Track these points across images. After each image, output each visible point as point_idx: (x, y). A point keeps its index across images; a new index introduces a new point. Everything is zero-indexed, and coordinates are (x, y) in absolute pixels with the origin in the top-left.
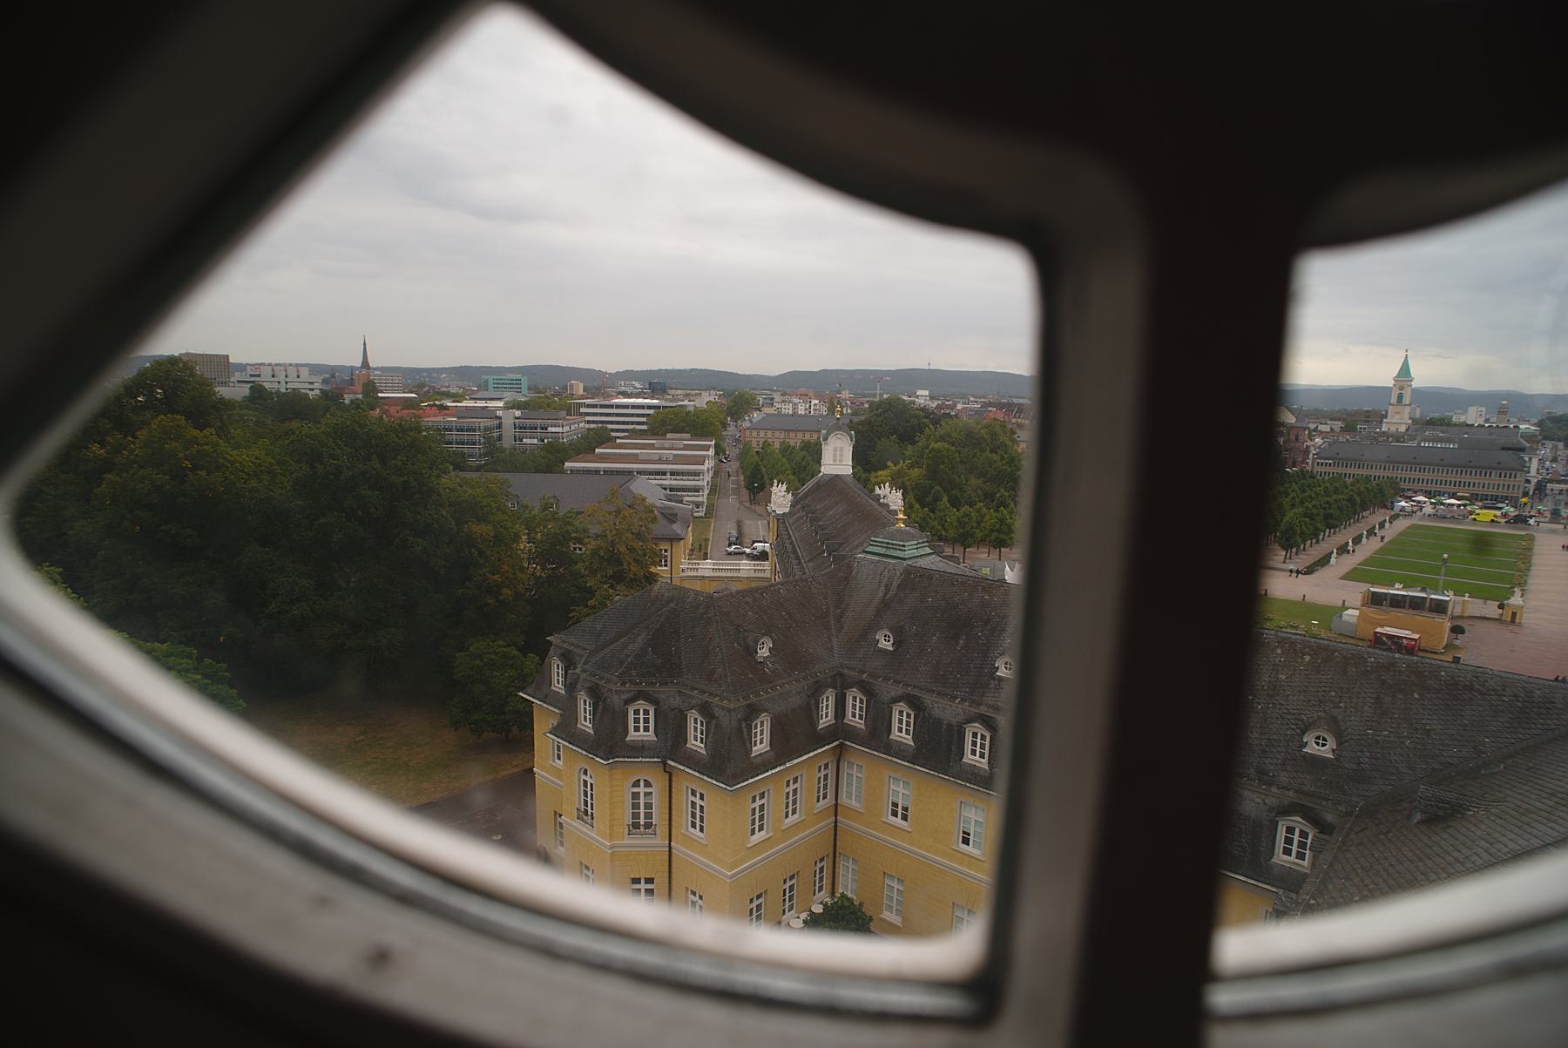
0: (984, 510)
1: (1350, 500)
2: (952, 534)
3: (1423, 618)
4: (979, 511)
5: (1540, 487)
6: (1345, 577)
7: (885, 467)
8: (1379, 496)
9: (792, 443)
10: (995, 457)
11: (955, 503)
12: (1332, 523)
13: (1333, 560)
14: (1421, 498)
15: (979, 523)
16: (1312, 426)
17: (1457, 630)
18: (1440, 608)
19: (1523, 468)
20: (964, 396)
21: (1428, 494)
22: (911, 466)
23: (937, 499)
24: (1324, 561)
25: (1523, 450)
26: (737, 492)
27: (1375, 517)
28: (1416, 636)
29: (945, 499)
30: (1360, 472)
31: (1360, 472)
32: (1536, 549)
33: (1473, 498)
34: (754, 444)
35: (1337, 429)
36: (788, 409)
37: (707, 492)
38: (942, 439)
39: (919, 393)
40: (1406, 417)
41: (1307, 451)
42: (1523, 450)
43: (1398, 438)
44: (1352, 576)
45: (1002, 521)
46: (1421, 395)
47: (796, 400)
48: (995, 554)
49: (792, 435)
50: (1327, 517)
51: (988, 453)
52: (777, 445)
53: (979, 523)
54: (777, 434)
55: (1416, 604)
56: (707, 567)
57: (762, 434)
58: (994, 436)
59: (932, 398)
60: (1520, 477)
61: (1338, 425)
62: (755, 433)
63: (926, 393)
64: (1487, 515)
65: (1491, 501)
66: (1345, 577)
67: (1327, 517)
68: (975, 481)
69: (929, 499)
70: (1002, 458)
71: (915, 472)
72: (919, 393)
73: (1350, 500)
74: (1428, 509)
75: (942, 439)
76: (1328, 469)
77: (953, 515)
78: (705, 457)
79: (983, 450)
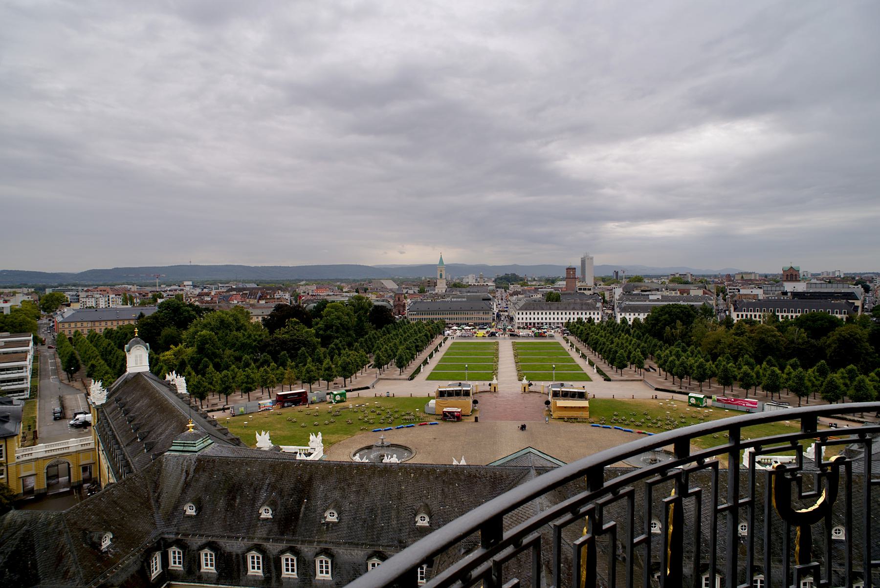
0: (236, 370)
1: (426, 335)
2: (218, 388)
3: (462, 400)
4: (233, 370)
5: (498, 316)
6: (428, 379)
7: (168, 349)
8: (438, 329)
9: (98, 331)
10: (240, 335)
11: (218, 367)
12: (419, 349)
14: (455, 328)
15: (233, 378)
16: (405, 291)
17: (475, 402)
18: (467, 394)
19: (491, 309)
20: (214, 283)
21: (458, 325)
22: (187, 346)
23: (206, 366)
24: (418, 371)
25: (490, 299)
26: (56, 372)
27: (438, 340)
28: (459, 410)
29: (211, 366)
32: (501, 349)
33: (475, 325)
34: (66, 333)
35: (416, 291)
36: (91, 303)
37: (29, 379)
38: (205, 326)
39: (186, 283)
41: (404, 306)
42: (490, 299)
43: (443, 297)
45: (248, 376)
46: (451, 268)
47: (98, 296)
48: (245, 396)
49: (97, 324)
50: (417, 346)
51: (235, 333)
52: (86, 331)
53: (233, 378)
54: (85, 324)
55: (458, 393)
56: (40, 450)
57: (73, 325)
58: (237, 320)
60: (491, 313)
61: (416, 289)
62: (66, 325)
63: (190, 283)
64: (481, 333)
65: (483, 325)
66: (428, 379)
67: (417, 346)
68: (228, 352)
69: (201, 367)
70: (244, 335)
71: (190, 350)
72: (186, 283)
73: (426, 335)
74: (458, 333)
75: (205, 326)
77: (218, 376)
78: (26, 352)
79: (231, 330)
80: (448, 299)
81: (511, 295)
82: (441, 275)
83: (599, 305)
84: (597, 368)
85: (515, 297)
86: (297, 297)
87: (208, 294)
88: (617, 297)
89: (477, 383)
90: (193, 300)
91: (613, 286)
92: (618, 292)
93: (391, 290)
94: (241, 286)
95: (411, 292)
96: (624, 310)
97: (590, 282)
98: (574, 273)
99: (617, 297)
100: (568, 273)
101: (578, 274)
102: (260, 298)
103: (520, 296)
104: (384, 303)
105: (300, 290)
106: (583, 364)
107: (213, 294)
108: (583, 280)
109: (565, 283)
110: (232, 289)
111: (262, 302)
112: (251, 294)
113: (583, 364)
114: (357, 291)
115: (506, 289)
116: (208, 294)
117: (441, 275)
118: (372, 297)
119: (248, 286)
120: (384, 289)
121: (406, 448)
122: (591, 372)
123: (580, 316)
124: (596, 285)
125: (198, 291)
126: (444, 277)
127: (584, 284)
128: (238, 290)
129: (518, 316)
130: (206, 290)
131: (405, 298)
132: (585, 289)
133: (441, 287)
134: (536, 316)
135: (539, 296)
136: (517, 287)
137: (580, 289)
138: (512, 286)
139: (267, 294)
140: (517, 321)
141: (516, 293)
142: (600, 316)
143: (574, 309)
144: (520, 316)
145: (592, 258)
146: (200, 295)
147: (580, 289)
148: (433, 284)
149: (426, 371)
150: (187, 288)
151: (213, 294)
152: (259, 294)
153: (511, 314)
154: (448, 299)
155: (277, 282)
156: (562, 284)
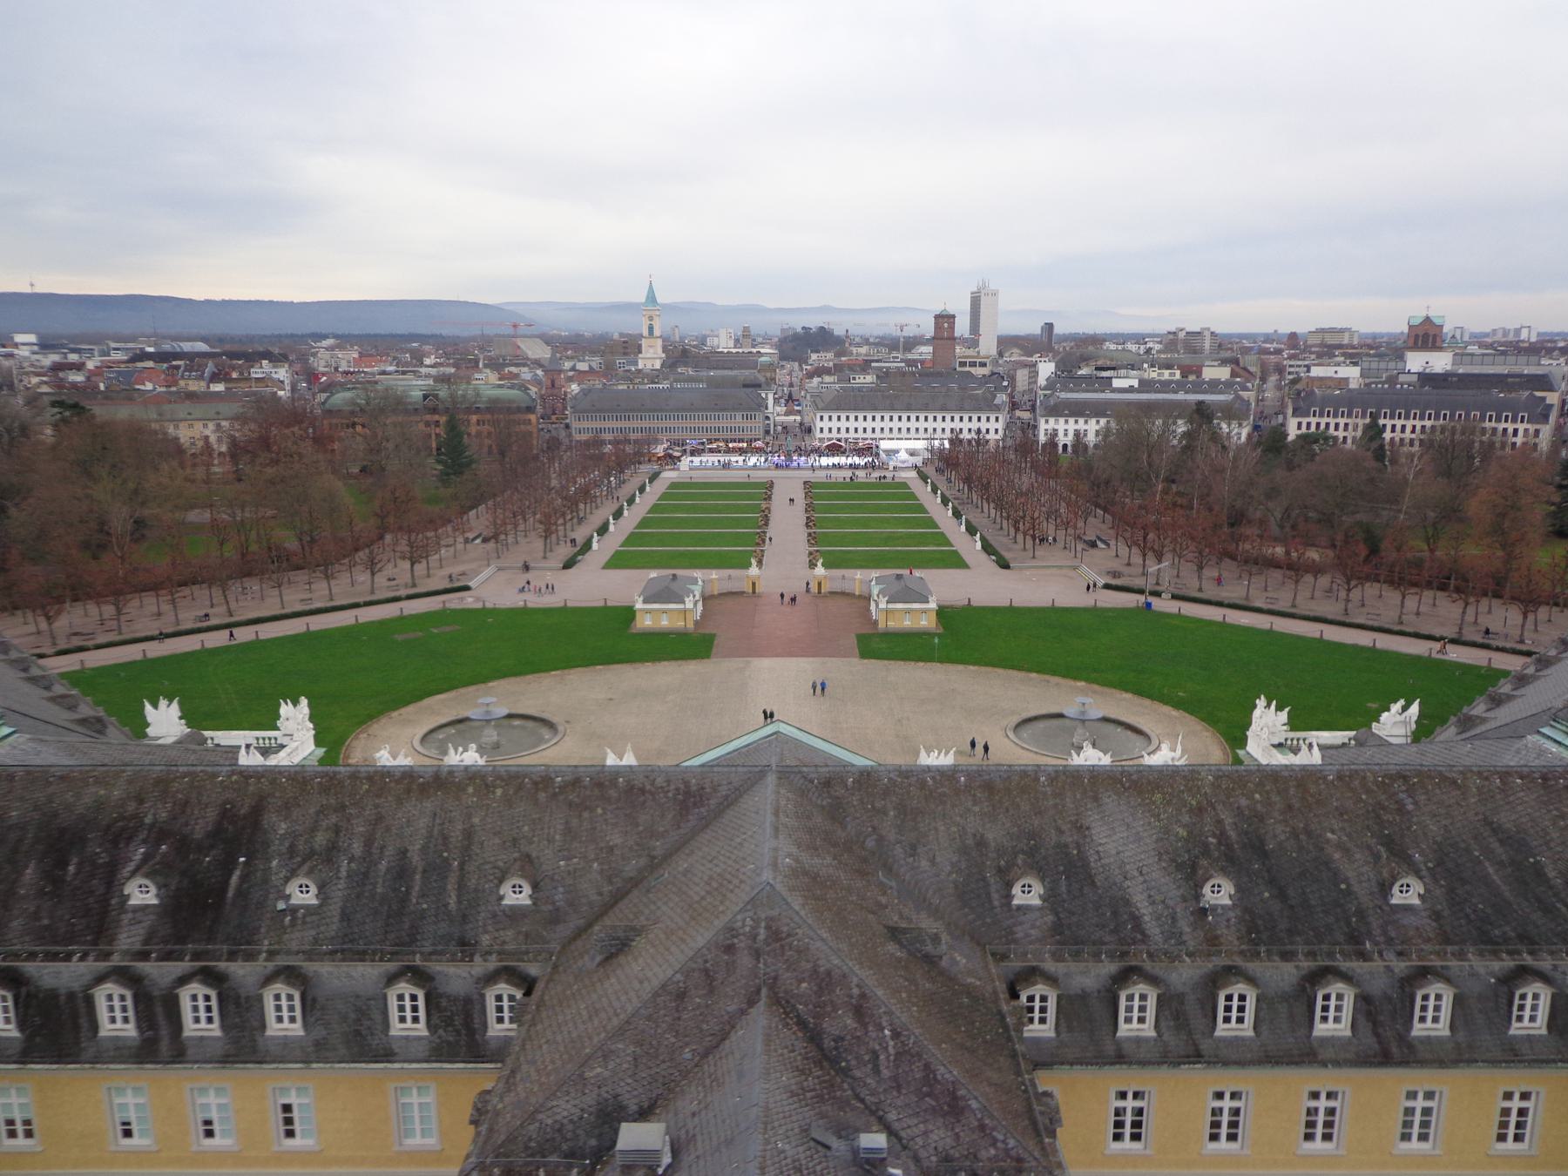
6: (607, 566)
13: (595, 546)
16: (567, 365)
20: (98, 339)
25: (759, 386)
30: (619, 424)
31: (619, 424)
39: (19, 338)
40: (660, 350)
42: (759, 386)
43: (654, 377)
44: (617, 561)
59: (45, 346)
60: (760, 417)
63: (32, 338)
66: (607, 566)
72: (19, 338)
76: (585, 424)
80: (665, 385)
81: (810, 375)
82: (651, 328)
83: (1002, 398)
84: (983, 539)
85: (816, 380)
86: (312, 377)
87: (79, 367)
88: (1042, 381)
89: (714, 574)
90: (35, 380)
91: (1036, 357)
92: (1046, 369)
93: (538, 363)
94: (167, 347)
95: (583, 366)
96: (1056, 411)
97: (988, 346)
98: (952, 327)
99: (1042, 381)
100: (938, 327)
101: (962, 327)
102: (215, 378)
103: (827, 379)
104: (514, 393)
105: (320, 363)
106: (955, 531)
107: (90, 365)
108: (973, 343)
109: (930, 349)
110: (144, 356)
111: (219, 387)
112: (189, 369)
113: (955, 531)
114: (456, 365)
115: (803, 360)
116: (79, 367)
117: (651, 328)
118: (486, 383)
119: (187, 347)
120: (522, 361)
121: (550, 725)
122: (971, 549)
123: (957, 425)
124: (1001, 354)
125: (54, 358)
126: (657, 332)
127: (971, 352)
128: (160, 357)
129: (819, 424)
130: (73, 357)
131: (570, 379)
132: (973, 364)
133: (651, 357)
134: (861, 424)
135: (870, 378)
136: (826, 358)
137: (963, 364)
138: (814, 356)
139: (233, 368)
140: (818, 435)
141: (820, 372)
142: (1000, 426)
143: (943, 409)
144: (826, 424)
145: (995, 294)
146: (57, 368)
147: (963, 364)
148: (630, 346)
149: (601, 549)
150: (24, 352)
151: (90, 365)
152: (210, 367)
153: (807, 420)
154: (665, 385)
155: (251, 339)
156: (926, 351)
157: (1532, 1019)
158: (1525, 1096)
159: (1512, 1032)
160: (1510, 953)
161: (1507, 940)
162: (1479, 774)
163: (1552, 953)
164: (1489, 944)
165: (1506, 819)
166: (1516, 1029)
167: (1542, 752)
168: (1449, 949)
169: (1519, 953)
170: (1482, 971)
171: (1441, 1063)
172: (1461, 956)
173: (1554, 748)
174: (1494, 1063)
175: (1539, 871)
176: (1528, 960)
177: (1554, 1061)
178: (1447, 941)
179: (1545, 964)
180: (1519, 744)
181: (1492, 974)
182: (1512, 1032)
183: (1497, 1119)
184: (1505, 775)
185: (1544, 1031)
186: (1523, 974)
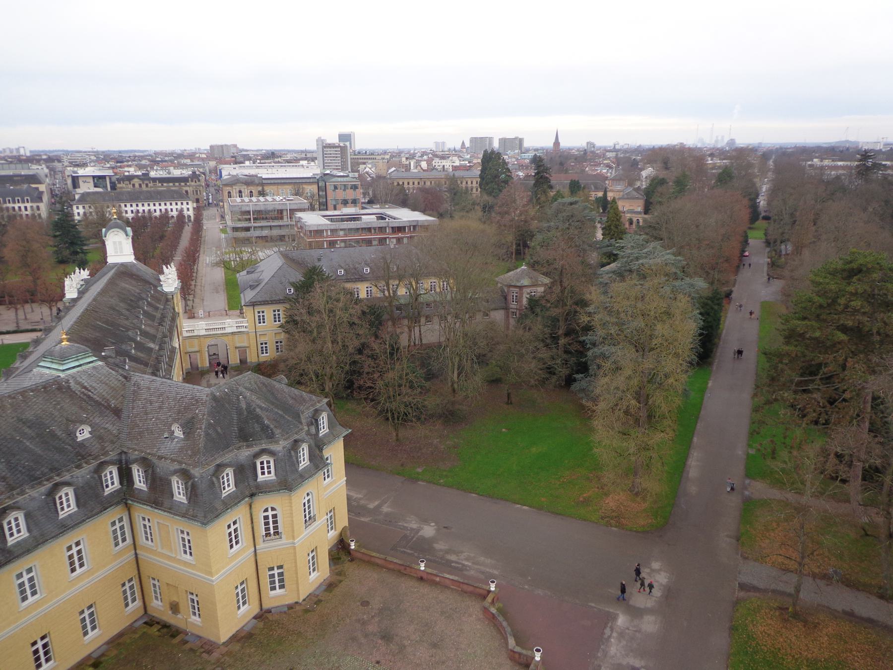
157: (69, 506)
158: (78, 544)
159: (61, 517)
160: (48, 480)
161: (44, 475)
162: (9, 396)
163: (68, 471)
164: (35, 480)
165: (29, 415)
166: (62, 515)
167: (42, 375)
168: (15, 492)
169: (52, 478)
170: (36, 495)
171: (28, 551)
172: (22, 493)
173: (47, 371)
174: (56, 536)
175: (53, 435)
176: (58, 479)
177: (84, 521)
178: (13, 489)
179: (67, 477)
180: (30, 375)
181: (42, 495)
182: (61, 517)
183: (68, 562)
184: (23, 393)
185: (76, 509)
186: (57, 487)
